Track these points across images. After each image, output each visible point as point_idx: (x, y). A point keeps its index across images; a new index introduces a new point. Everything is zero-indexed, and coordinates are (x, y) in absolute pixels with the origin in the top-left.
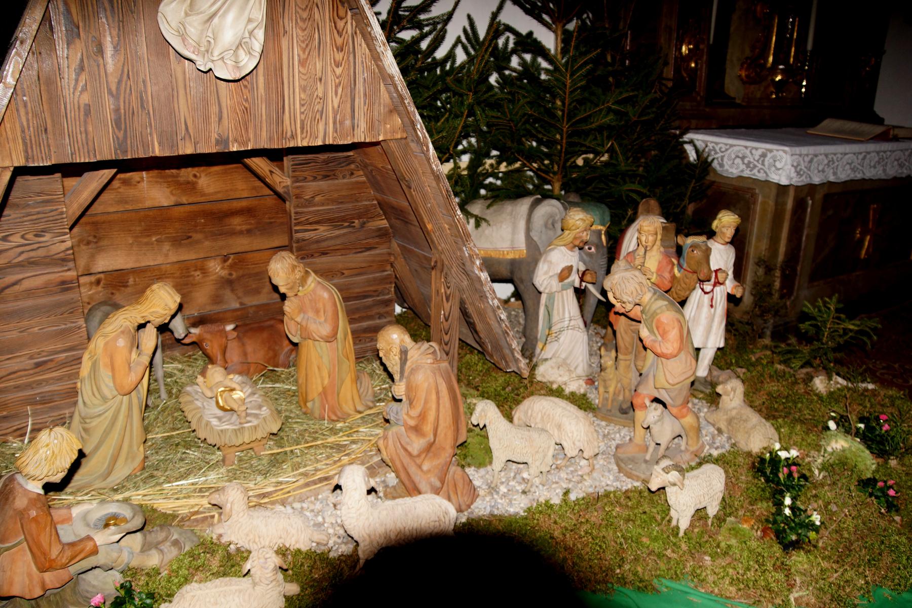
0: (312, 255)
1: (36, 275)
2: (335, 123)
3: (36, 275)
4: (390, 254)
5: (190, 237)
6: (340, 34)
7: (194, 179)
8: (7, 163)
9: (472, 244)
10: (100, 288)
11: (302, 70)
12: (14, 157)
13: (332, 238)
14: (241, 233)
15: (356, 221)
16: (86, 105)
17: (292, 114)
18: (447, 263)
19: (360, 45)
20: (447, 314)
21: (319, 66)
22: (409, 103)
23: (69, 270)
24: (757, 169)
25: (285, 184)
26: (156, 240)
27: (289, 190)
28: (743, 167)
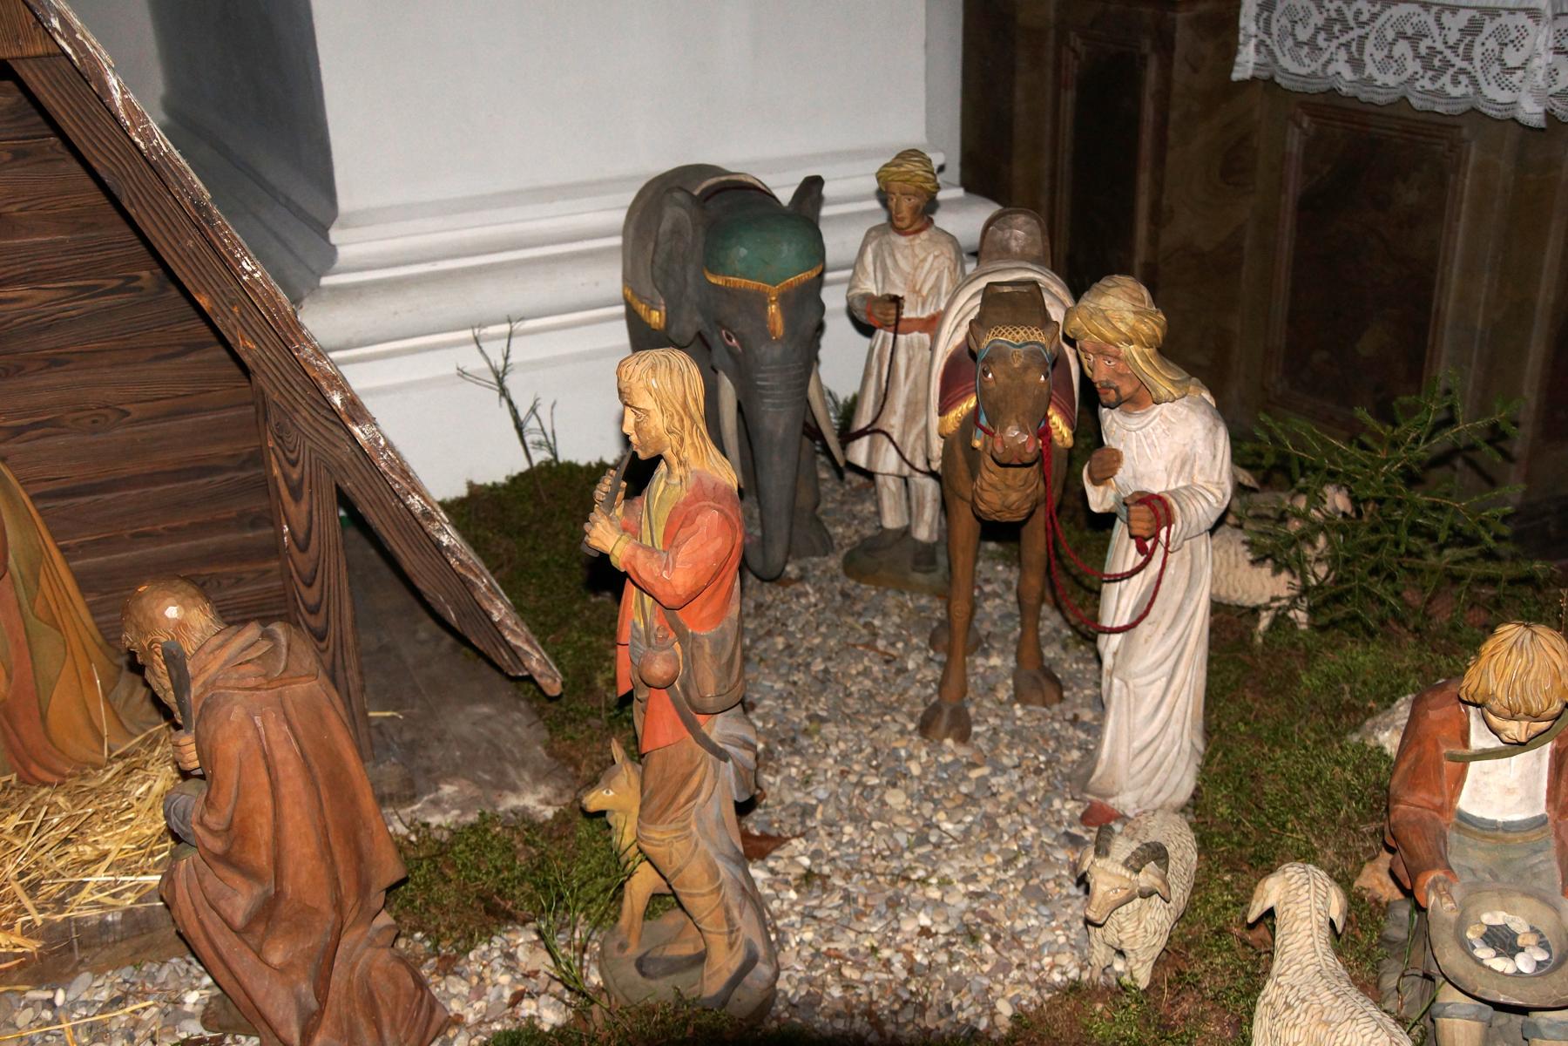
9: (309, 350)
18: (276, 397)
20: (301, 535)
24: (1451, 71)
28: (1413, 66)
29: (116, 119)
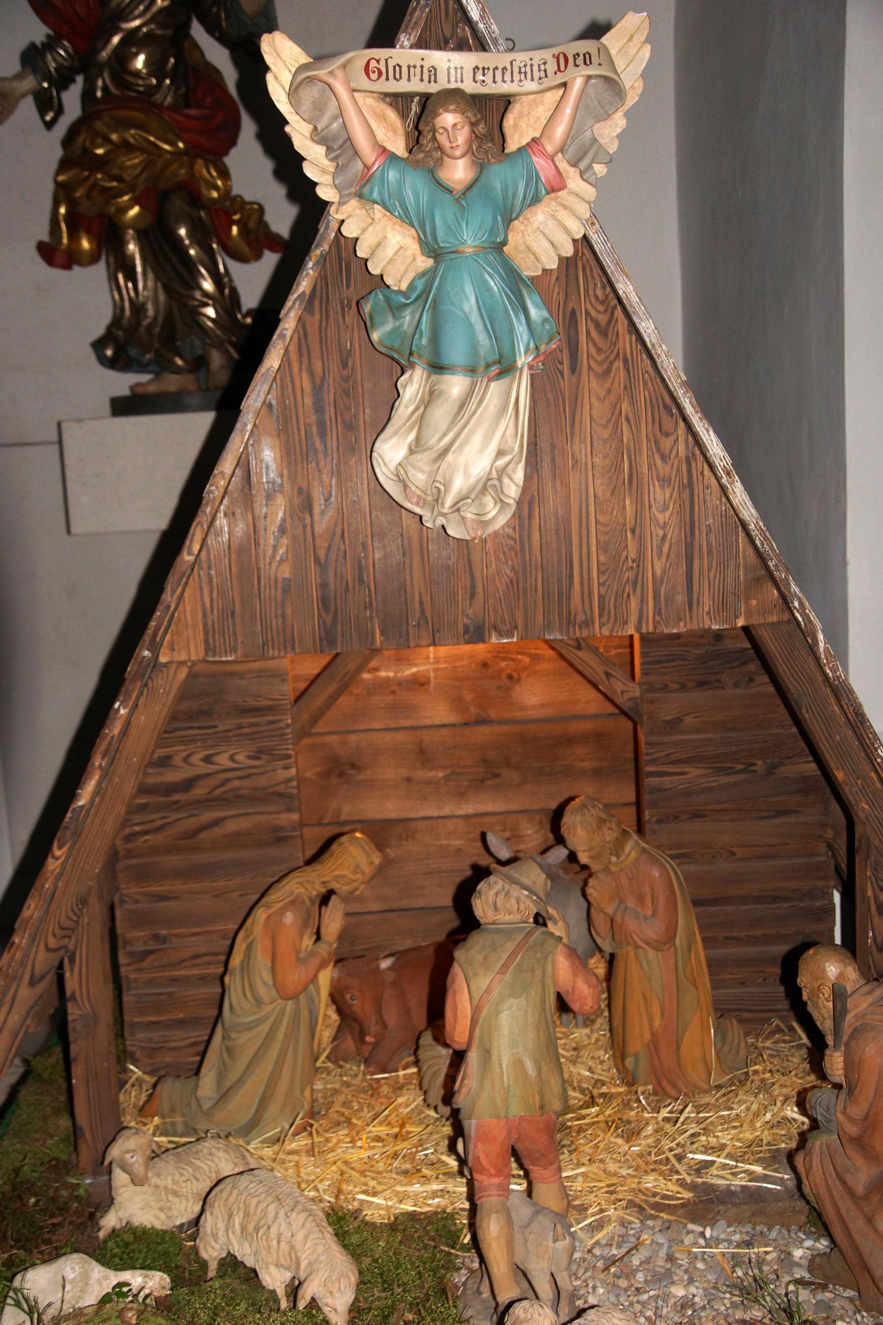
0: (676, 818)
1: (238, 816)
2: (656, 597)
3: (238, 816)
4: (824, 825)
6: (663, 457)
8: (183, 657)
12: (192, 649)
15: (760, 763)
16: (284, 579)
17: (586, 586)
18: (877, 842)
19: (702, 473)
22: (776, 566)
25: (630, 695)
29: (817, 659)
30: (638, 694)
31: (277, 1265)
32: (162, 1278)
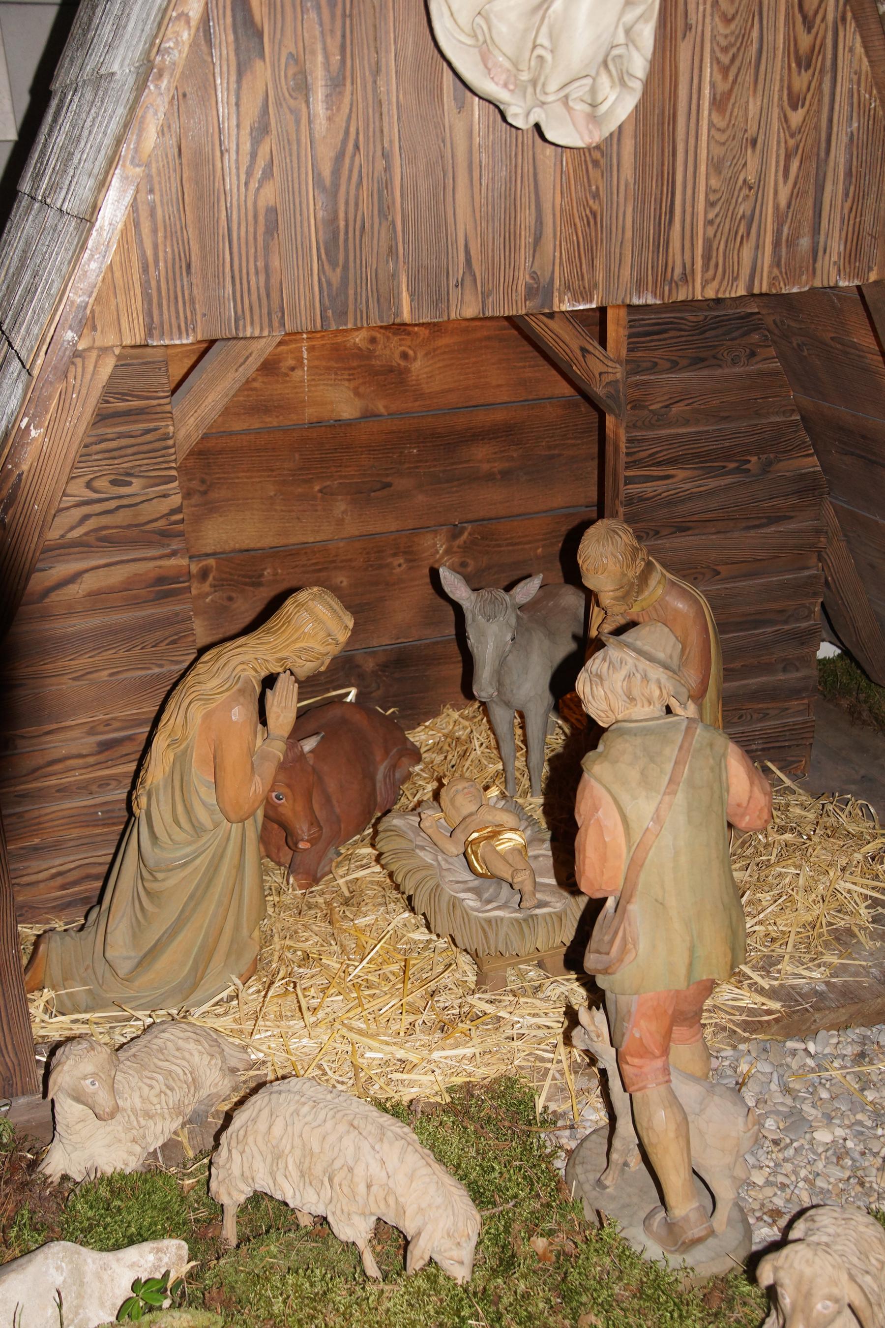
0: (657, 533)
4: (818, 532)
5: (389, 485)
7: (403, 363)
8: (111, 339)
10: (206, 587)
11: (716, 118)
12: (125, 325)
13: (700, 495)
14: (490, 477)
15: (754, 459)
21: (753, 109)
23: (174, 554)
25: (611, 378)
26: (320, 491)
27: (618, 391)
30: (619, 376)
31: (363, 1214)
32: (179, 1247)
